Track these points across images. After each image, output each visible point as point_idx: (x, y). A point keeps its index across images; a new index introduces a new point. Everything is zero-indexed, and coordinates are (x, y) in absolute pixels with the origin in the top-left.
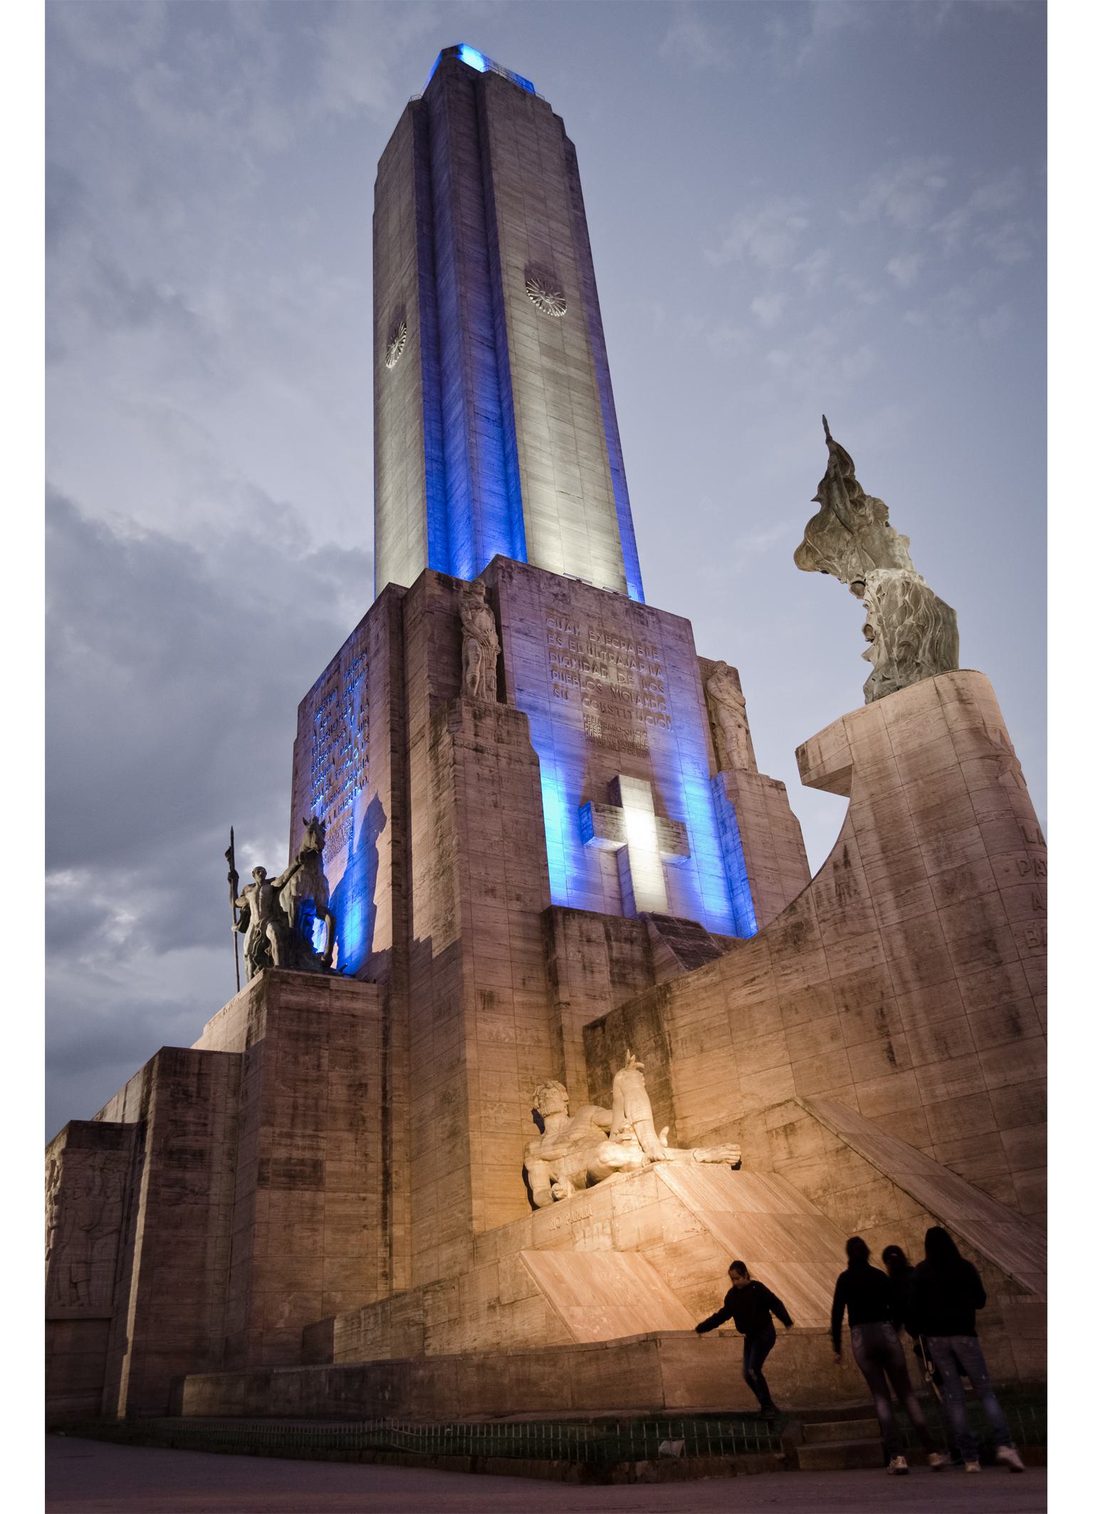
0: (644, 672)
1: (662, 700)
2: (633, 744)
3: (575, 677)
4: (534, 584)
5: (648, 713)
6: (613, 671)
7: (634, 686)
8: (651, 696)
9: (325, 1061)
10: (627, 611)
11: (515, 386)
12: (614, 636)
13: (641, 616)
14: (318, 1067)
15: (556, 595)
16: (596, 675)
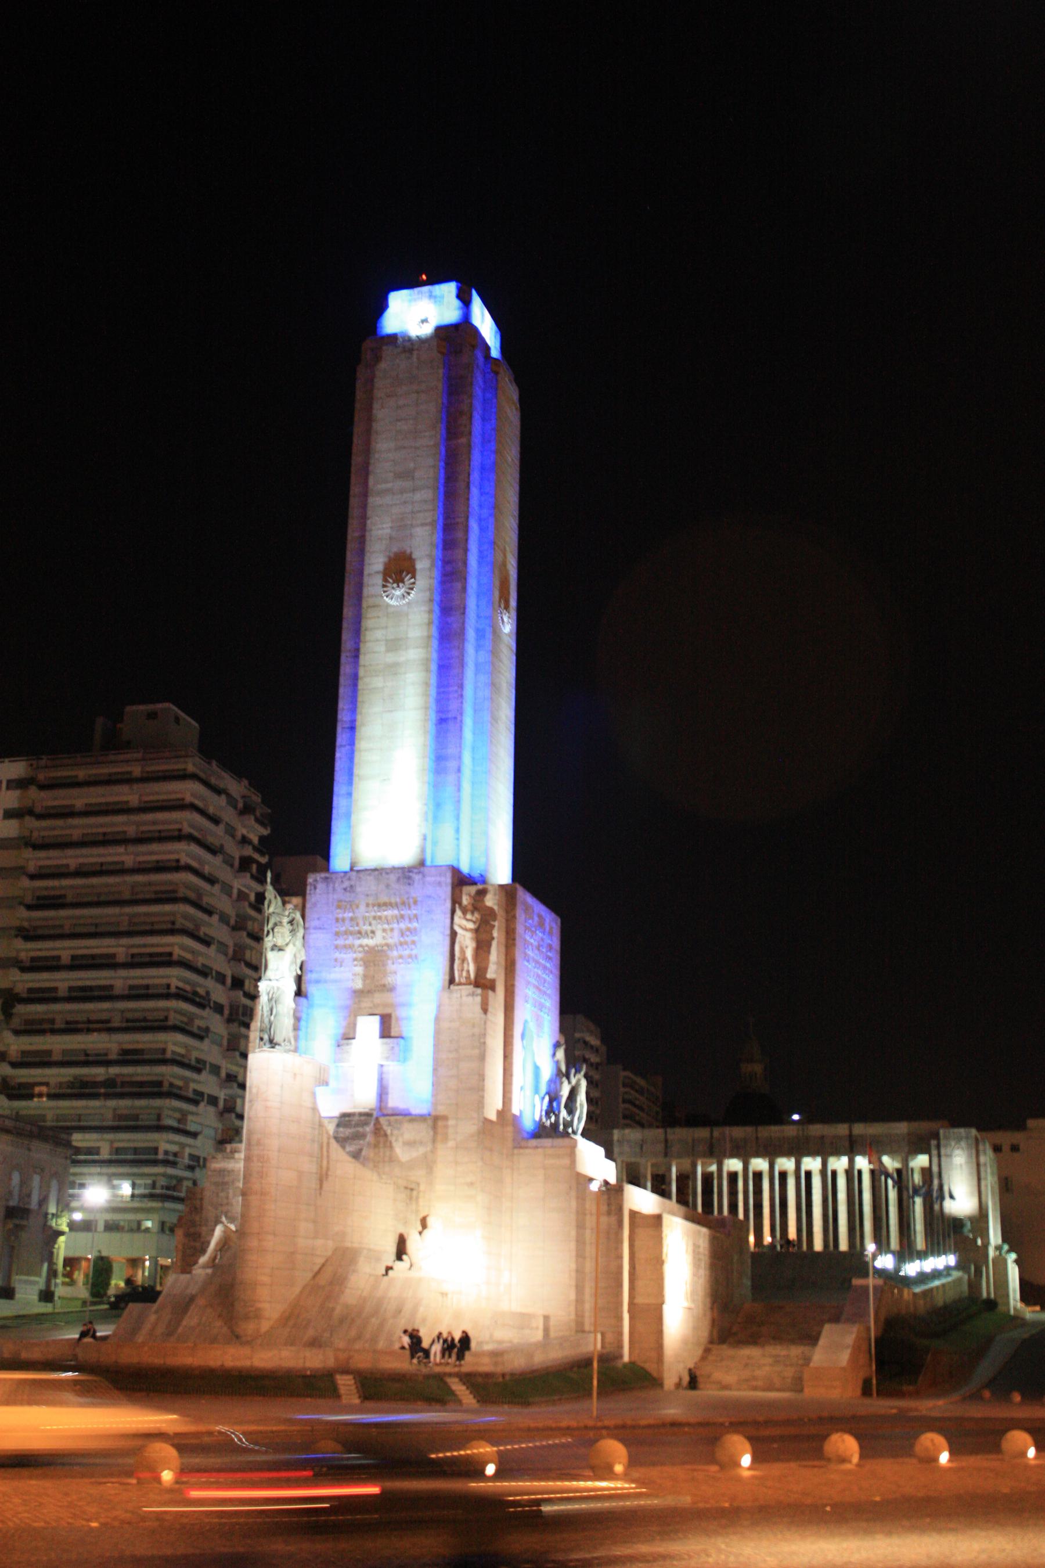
0: (403, 925)
1: (414, 943)
2: (384, 986)
3: (350, 947)
4: (331, 885)
5: (401, 957)
6: (379, 934)
7: (394, 939)
8: (406, 943)
9: (231, 1195)
10: (398, 879)
11: (360, 699)
12: (385, 904)
13: (409, 878)
14: (227, 1198)
15: (345, 889)
16: (365, 941)
